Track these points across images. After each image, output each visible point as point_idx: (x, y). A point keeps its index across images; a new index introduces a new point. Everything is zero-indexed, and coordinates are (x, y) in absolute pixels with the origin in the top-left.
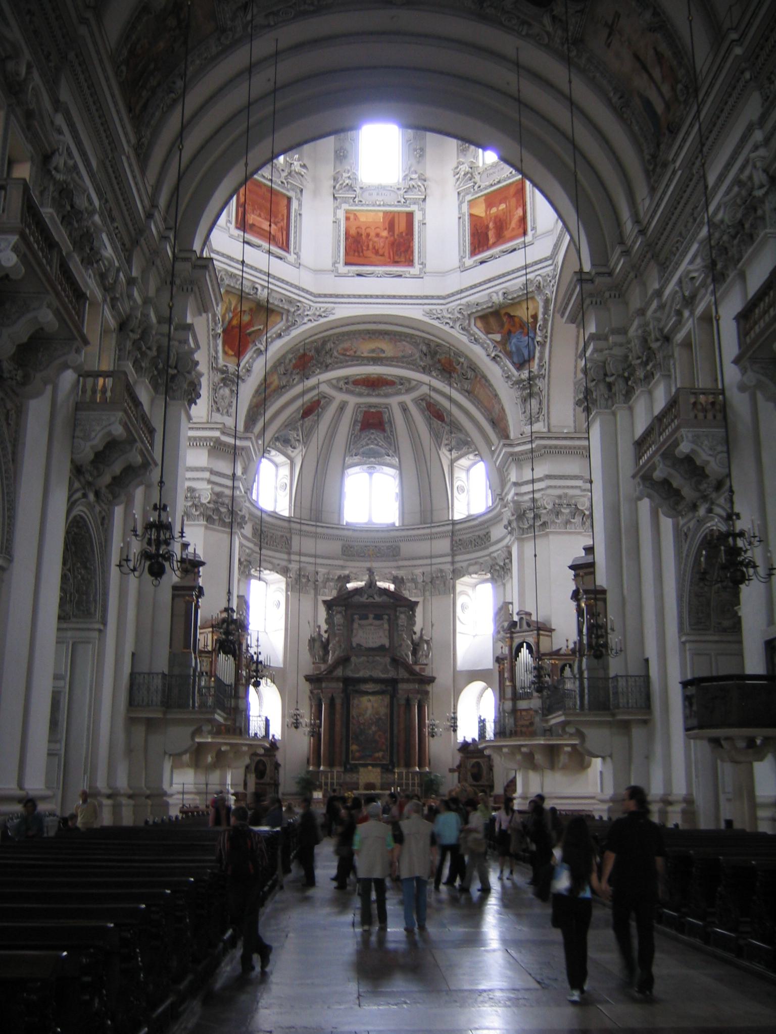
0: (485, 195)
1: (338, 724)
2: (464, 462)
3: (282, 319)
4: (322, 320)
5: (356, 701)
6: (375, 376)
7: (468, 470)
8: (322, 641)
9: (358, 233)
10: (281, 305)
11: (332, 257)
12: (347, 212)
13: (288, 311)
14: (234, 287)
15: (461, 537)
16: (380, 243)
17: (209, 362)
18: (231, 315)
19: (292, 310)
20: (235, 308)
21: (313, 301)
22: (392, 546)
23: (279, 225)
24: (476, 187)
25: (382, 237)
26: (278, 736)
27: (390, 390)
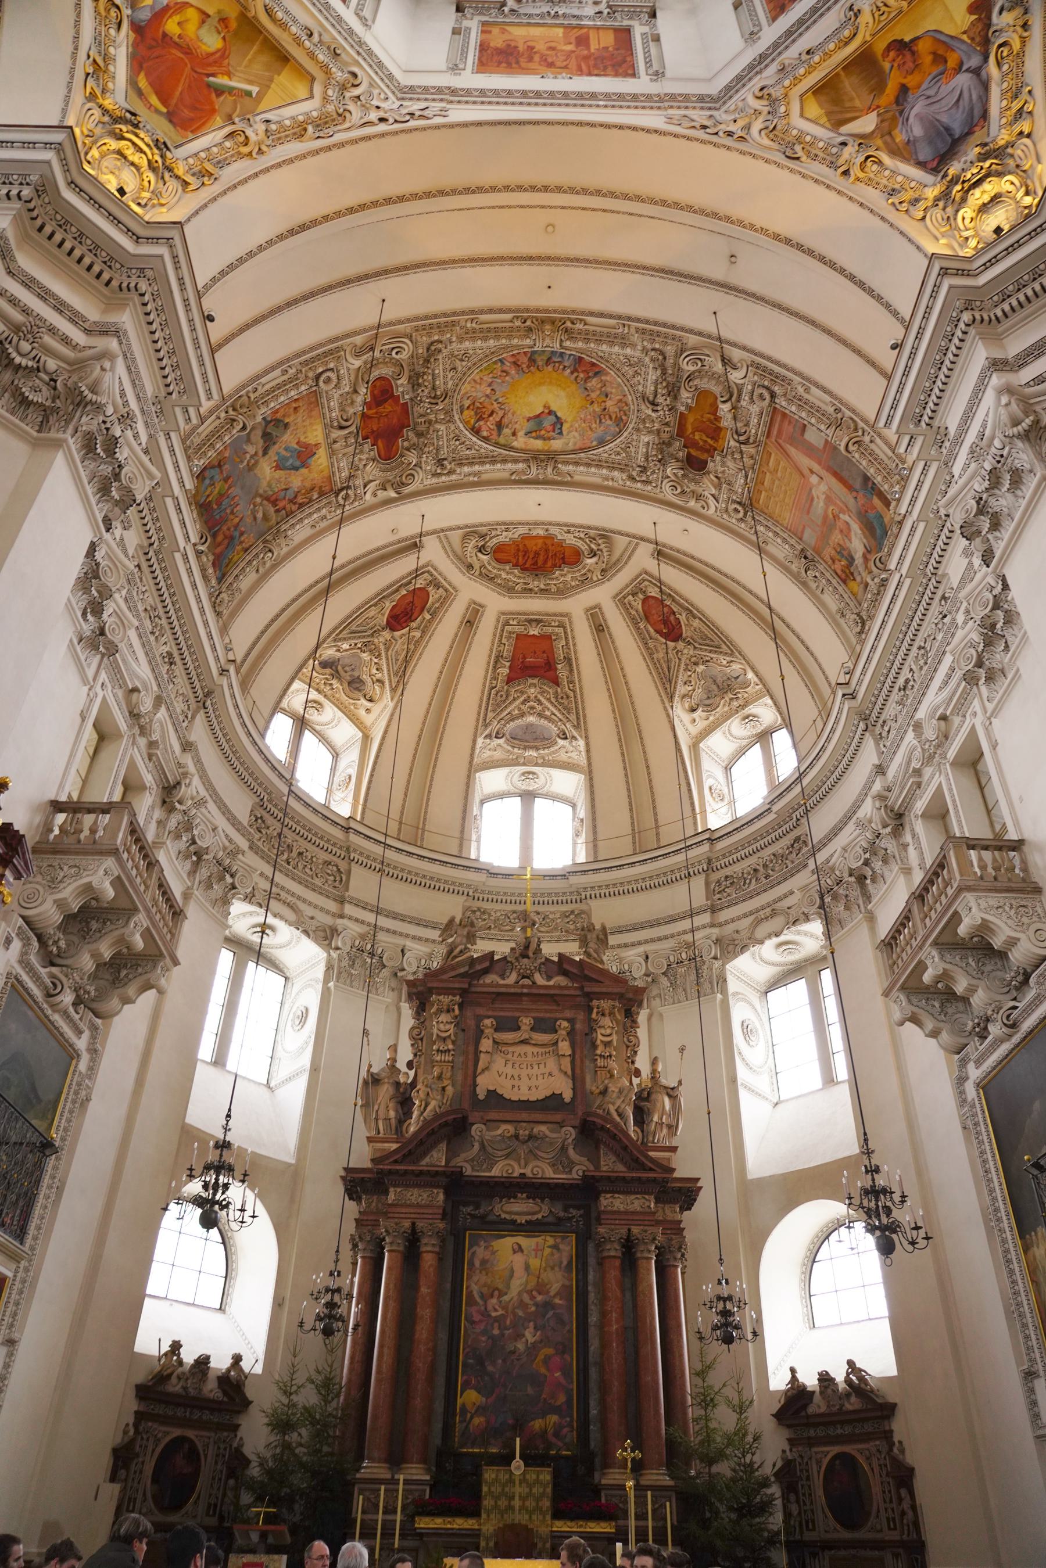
1: (425, 1313)
2: (719, 744)
3: (312, 97)
4: (413, 123)
5: (480, 1252)
6: (541, 533)
7: (728, 769)
8: (398, 1084)
9: (509, 46)
10: (307, 44)
12: (484, 24)
15: (728, 871)
19: (339, 75)
22: (572, 912)
26: (254, 1363)
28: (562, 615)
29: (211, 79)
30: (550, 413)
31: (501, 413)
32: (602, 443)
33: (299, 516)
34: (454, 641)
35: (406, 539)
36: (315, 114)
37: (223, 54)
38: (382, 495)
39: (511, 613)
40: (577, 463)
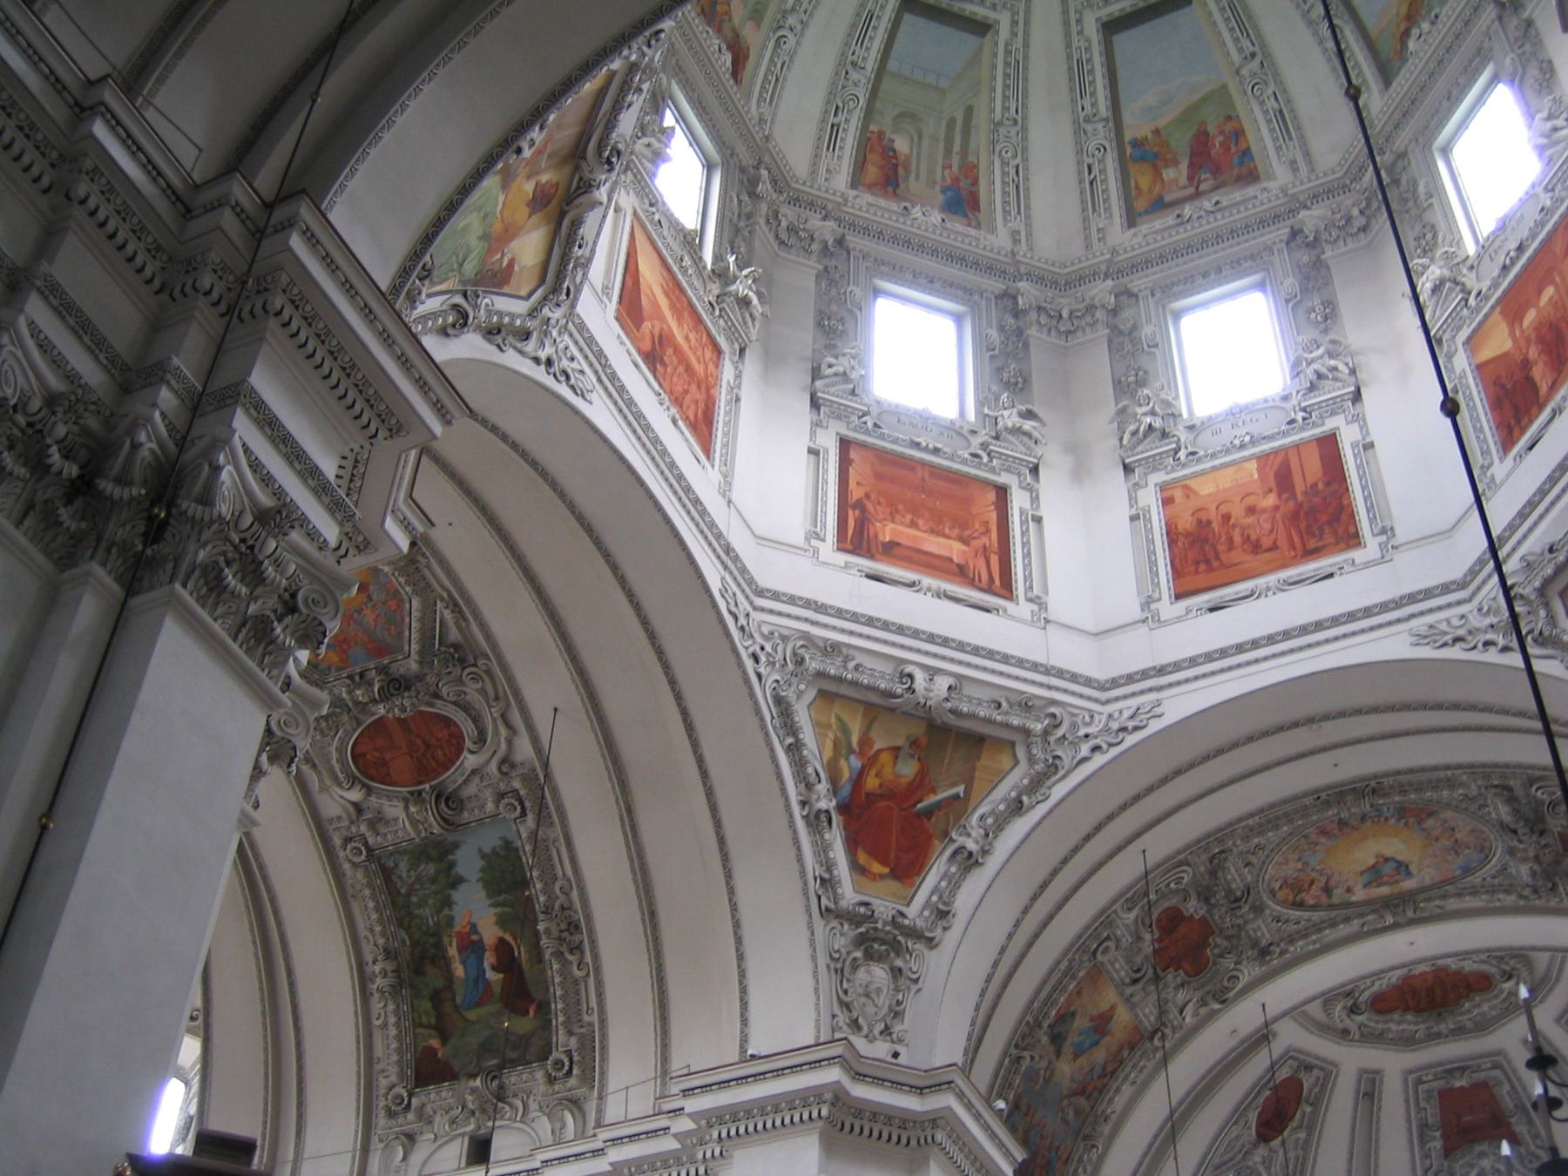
0: (1499, 301)
3: (1017, 762)
4: (1131, 740)
6: (1427, 969)
9: (1199, 522)
10: (999, 718)
11: (1139, 593)
12: (1163, 487)
13: (1026, 732)
14: (840, 680)
16: (1261, 527)
17: (806, 894)
18: (856, 763)
19: (1038, 727)
20: (865, 741)
21: (1097, 701)
23: (977, 543)
24: (1472, 302)
25: (1264, 511)
27: (1484, 1006)
28: (1490, 1054)
29: (919, 806)
30: (1387, 860)
31: (1323, 880)
32: (1467, 870)
33: (1114, 1087)
34: (1354, 1126)
35: (1251, 1036)
36: (1026, 781)
37: (922, 774)
38: (1203, 1011)
39: (1420, 1069)
40: (1444, 897)
